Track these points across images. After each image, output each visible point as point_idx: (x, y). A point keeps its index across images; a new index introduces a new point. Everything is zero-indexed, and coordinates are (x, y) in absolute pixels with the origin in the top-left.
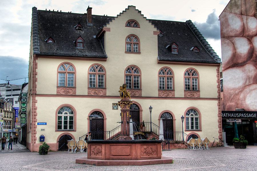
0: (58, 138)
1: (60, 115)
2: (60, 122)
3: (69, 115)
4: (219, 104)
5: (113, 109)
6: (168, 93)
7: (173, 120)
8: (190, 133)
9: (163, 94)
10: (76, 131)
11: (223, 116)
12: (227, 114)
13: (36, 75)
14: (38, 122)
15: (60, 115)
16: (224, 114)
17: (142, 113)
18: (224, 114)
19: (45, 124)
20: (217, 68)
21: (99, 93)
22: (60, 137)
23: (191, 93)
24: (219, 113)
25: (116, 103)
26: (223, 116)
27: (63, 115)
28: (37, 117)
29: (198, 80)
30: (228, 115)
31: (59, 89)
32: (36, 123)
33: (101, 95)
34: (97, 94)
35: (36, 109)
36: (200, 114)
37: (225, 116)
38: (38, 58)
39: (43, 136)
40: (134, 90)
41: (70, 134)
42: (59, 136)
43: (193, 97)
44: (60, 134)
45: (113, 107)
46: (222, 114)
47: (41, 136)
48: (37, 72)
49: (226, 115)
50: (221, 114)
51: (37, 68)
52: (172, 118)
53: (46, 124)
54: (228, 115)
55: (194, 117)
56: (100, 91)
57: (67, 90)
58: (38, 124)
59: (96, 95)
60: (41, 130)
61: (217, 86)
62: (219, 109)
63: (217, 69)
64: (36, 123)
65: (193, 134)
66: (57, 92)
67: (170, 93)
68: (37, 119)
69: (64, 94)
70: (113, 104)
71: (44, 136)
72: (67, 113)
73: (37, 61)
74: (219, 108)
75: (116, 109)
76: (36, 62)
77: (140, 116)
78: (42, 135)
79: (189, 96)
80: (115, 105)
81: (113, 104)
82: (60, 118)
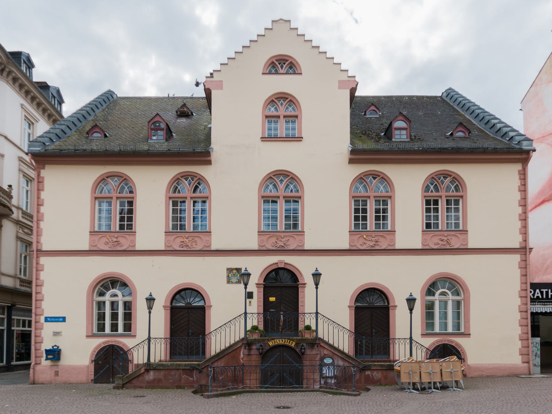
0: (92, 354)
1: (101, 299)
2: (101, 317)
3: (120, 299)
4: (523, 263)
5: (229, 282)
6: (377, 238)
7: (391, 308)
8: (437, 342)
9: (362, 241)
10: (135, 336)
11: (534, 295)
12: (544, 291)
13: (42, 205)
14: (47, 314)
15: (101, 299)
16: (538, 291)
17: (303, 292)
18: (538, 291)
19: (61, 319)
20: (519, 167)
21: (194, 244)
22: (97, 351)
23: (443, 238)
24: (521, 287)
25: (234, 267)
26: (534, 295)
27: (107, 298)
28: (44, 305)
29: (463, 203)
30: (547, 293)
31: (96, 238)
32: (42, 319)
33: (198, 248)
34: (187, 246)
35: (42, 286)
36: (466, 290)
37: (538, 297)
38: (47, 166)
39: (58, 347)
40: (282, 235)
41: (121, 343)
42: (96, 348)
43: (448, 247)
44: (98, 342)
45: (228, 276)
46: (531, 292)
47: (53, 347)
48: (43, 199)
49: (542, 293)
50: (529, 289)
51: (43, 190)
52: (386, 304)
53: (64, 319)
54: (547, 293)
55: (451, 297)
56: (196, 239)
57: (115, 240)
58: (46, 319)
59: (185, 249)
60: (52, 334)
61: (520, 215)
62: (524, 278)
63: (519, 171)
64: (42, 319)
65: (444, 344)
66: (91, 245)
67: (381, 239)
68: (43, 310)
69: (106, 248)
70: (228, 269)
71: (59, 348)
72: (116, 295)
73: (43, 173)
74: (522, 275)
75: (236, 283)
76: (42, 175)
77: (300, 300)
78: (55, 346)
79: (435, 244)
80: (235, 271)
81: (228, 269)
82: (101, 305)
